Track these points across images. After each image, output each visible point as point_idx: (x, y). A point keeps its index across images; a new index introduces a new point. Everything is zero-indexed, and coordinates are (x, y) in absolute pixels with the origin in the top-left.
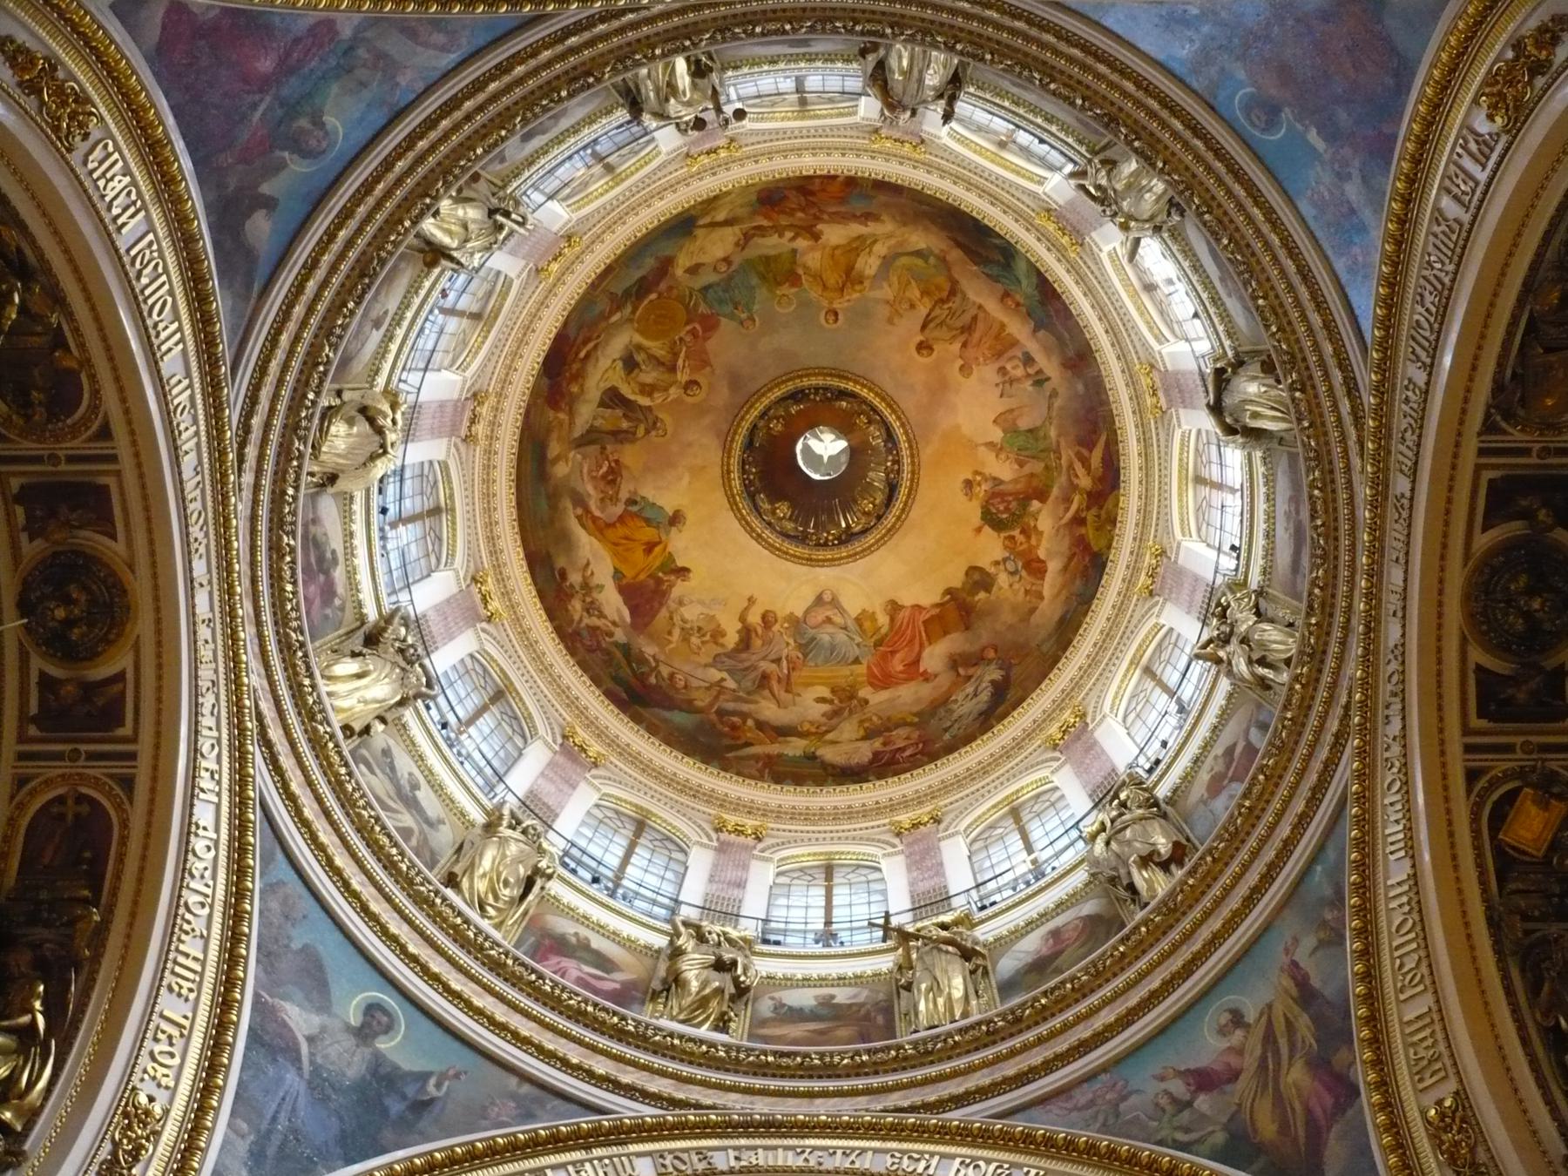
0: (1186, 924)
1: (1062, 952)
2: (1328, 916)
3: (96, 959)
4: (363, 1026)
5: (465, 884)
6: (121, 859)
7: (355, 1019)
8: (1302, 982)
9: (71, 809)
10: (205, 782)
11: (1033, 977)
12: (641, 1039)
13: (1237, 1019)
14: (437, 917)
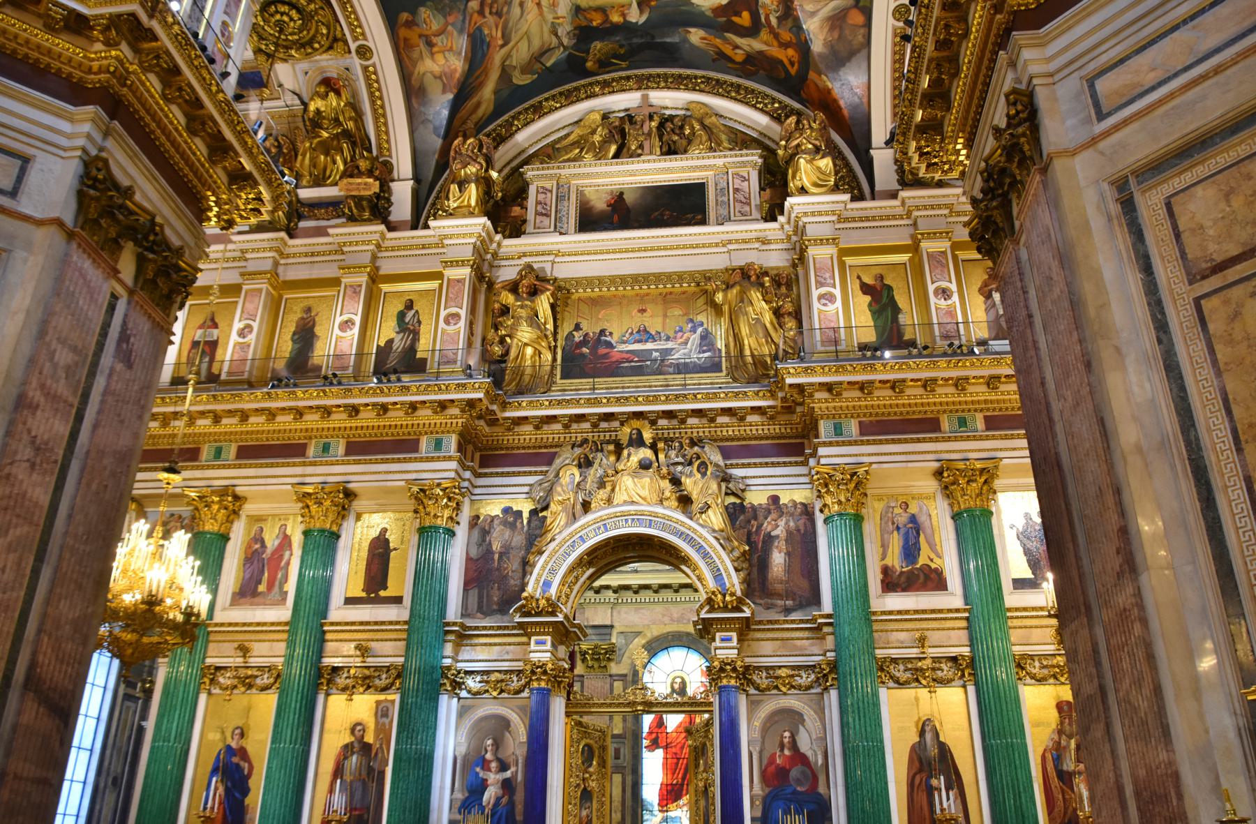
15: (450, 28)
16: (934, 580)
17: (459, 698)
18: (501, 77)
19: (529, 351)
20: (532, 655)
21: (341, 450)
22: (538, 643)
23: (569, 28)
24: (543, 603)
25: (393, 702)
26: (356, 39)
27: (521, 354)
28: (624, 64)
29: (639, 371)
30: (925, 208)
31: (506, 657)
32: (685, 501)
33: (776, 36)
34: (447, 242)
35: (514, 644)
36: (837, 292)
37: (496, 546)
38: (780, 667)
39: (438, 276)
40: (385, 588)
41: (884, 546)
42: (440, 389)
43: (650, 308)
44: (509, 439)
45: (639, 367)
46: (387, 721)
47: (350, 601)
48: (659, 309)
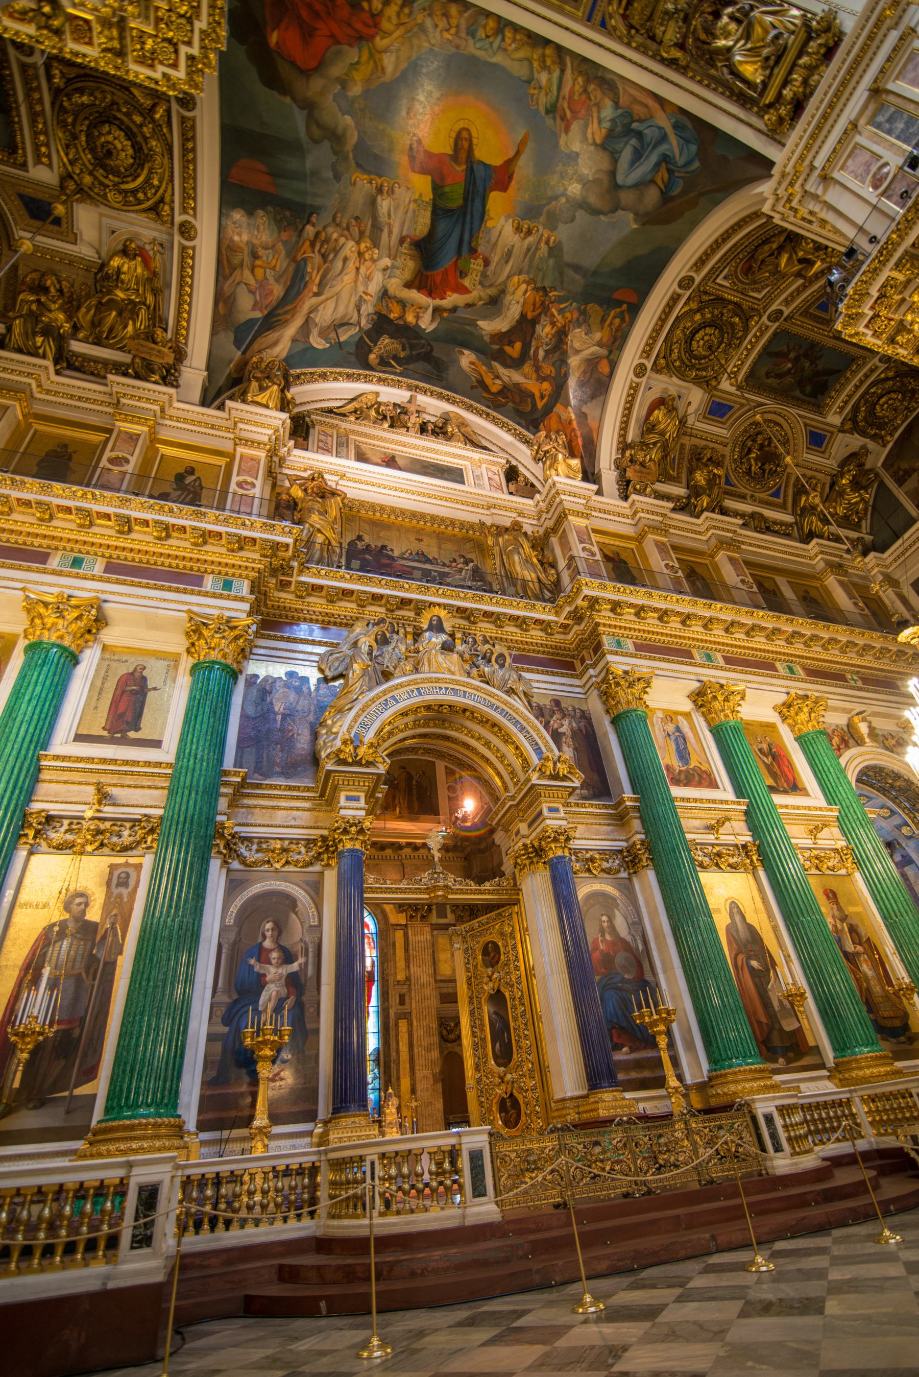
15: (280, 246)
17: (229, 871)
18: (302, 327)
20: (343, 812)
21: (98, 568)
22: (348, 798)
23: (371, 309)
25: (139, 867)
26: (184, 211)
28: (399, 369)
30: (648, 512)
31: (293, 823)
33: (537, 368)
34: (240, 425)
35: (303, 809)
37: (279, 707)
38: (587, 850)
40: (137, 729)
42: (244, 524)
46: (125, 892)
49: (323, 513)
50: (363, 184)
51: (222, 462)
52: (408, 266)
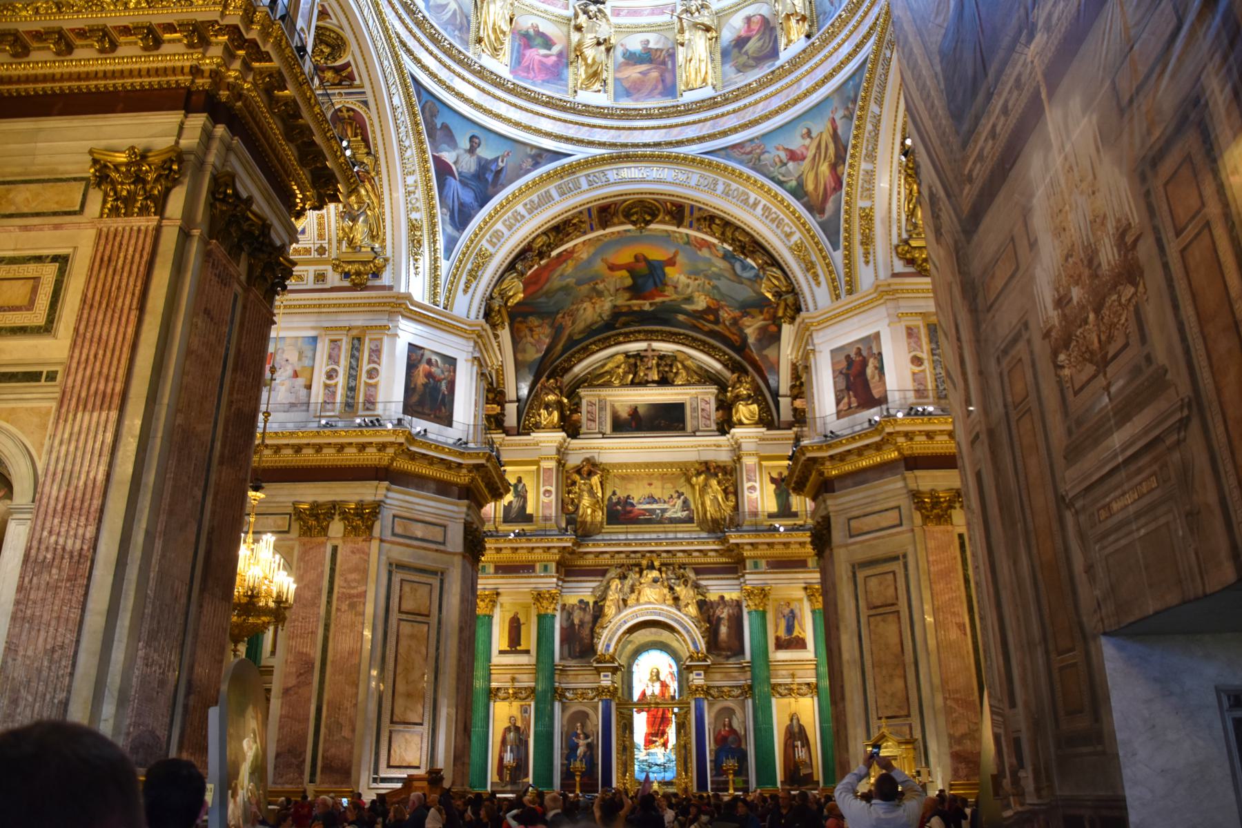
0: (797, 73)
1: (748, 39)
2: (850, 106)
3: (378, 173)
4: (472, 146)
5: (486, 39)
6: (373, 132)
7: (468, 146)
8: (835, 130)
9: (346, 114)
10: (393, 90)
11: (736, 50)
12: (573, 109)
13: (809, 134)
14: (482, 78)
16: (800, 644)
19: (589, 511)
21: (492, 570)
24: (607, 657)
27: (585, 513)
29: (649, 521)
32: (676, 599)
36: (757, 485)
37: (576, 621)
39: (536, 463)
41: (777, 626)
43: (655, 482)
44: (580, 562)
45: (649, 519)
47: (501, 652)
48: (658, 484)
49: (591, 492)
50: (585, 289)
51: (535, 468)
52: (627, 295)
